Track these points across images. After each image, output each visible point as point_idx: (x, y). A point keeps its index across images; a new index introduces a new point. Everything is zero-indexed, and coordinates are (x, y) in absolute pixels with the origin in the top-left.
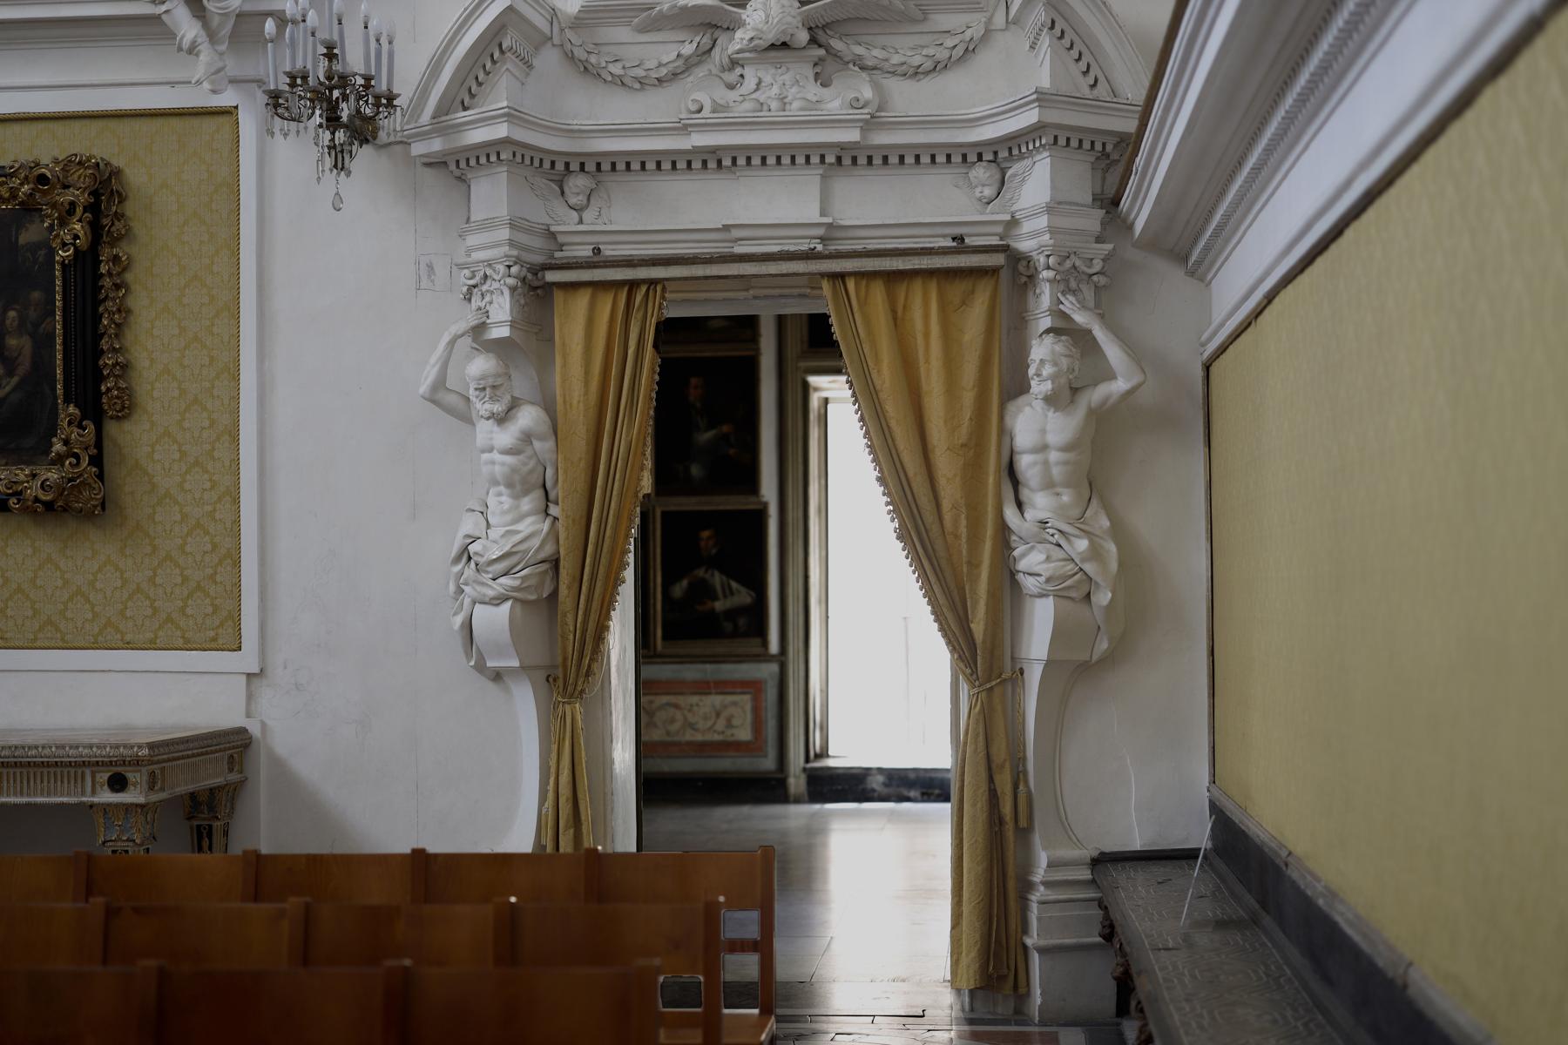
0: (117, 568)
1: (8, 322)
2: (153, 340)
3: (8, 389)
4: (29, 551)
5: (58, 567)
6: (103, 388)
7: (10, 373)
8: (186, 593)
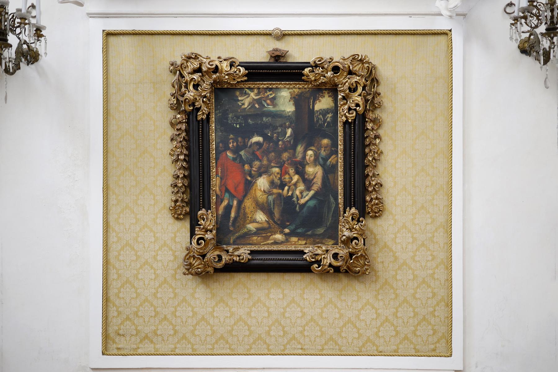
0: (373, 307)
1: (307, 158)
2: (396, 168)
3: (307, 198)
4: (318, 297)
5: (336, 307)
6: (368, 198)
7: (309, 189)
8: (416, 322)
